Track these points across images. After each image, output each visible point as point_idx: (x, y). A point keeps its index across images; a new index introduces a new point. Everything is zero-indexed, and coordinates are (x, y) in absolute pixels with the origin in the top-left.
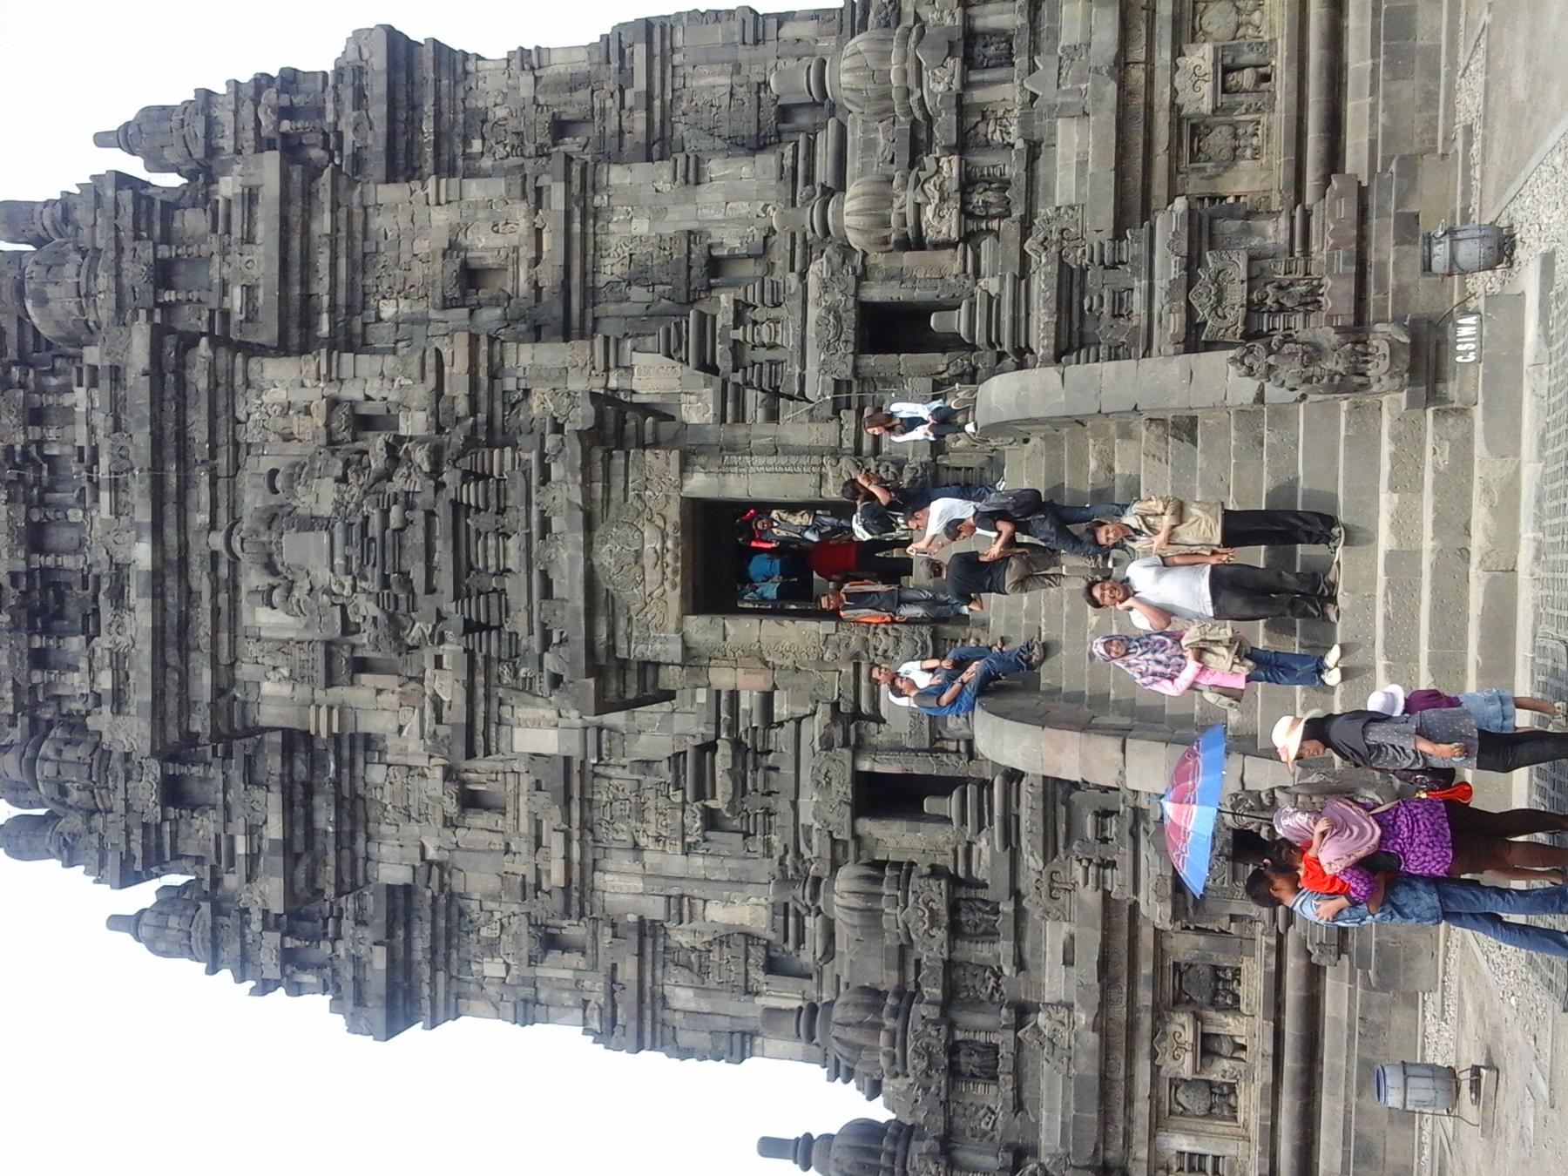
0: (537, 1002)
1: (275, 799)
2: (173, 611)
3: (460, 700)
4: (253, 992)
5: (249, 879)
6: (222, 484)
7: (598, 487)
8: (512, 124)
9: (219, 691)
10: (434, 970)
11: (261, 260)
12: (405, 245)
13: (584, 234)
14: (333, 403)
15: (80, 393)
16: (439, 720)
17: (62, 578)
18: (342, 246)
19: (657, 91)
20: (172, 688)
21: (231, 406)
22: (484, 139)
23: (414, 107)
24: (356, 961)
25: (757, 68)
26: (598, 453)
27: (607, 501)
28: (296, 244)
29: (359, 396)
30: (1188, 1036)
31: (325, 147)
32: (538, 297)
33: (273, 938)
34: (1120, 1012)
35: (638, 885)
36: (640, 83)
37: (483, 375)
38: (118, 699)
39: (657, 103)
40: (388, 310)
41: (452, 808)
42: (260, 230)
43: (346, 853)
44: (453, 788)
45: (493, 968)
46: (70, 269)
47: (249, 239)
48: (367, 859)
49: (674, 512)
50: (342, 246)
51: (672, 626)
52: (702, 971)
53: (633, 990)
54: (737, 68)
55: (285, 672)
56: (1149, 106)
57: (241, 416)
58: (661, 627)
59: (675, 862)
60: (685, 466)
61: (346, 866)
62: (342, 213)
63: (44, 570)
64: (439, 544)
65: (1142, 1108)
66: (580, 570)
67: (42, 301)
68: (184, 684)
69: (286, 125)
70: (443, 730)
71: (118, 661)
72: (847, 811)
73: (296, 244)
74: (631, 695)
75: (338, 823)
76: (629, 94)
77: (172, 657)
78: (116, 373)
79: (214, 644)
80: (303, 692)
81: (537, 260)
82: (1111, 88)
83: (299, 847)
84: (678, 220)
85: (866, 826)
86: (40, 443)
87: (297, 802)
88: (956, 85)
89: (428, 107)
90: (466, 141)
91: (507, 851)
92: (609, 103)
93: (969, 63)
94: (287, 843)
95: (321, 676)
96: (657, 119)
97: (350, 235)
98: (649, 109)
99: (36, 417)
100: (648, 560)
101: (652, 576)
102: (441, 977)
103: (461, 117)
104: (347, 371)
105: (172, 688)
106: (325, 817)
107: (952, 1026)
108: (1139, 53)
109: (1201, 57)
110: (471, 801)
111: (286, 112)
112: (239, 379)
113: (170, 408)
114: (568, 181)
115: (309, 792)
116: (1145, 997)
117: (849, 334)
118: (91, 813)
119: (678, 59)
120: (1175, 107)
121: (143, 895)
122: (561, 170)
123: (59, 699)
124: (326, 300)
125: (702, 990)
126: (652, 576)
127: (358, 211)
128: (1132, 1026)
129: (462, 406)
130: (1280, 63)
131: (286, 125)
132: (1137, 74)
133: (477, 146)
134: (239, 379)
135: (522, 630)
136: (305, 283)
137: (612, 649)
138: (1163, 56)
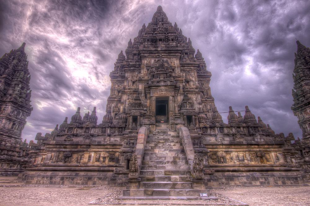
1: (134, 64)
2: (153, 52)
3: (144, 79)
4: (115, 63)
7: (170, 87)
8: (203, 87)
9: (145, 56)
10: (116, 80)
11: (188, 62)
12: (191, 76)
13: (193, 93)
14: (175, 67)
15: (175, 44)
16: (142, 77)
17: (157, 42)
18: (190, 70)
20: (145, 52)
21: (174, 57)
24: (118, 73)
26: (174, 87)
27: (169, 88)
30: (106, 155)
31: (199, 70)
32: (186, 89)
33: (120, 65)
34: (109, 147)
35: (125, 99)
36: (208, 100)
38: (144, 47)
40: (184, 74)
41: (133, 81)
42: (191, 62)
43: (128, 70)
44: (135, 81)
45: (116, 86)
46: (186, 45)
47: (190, 61)
48: (128, 73)
49: (167, 95)
50: (190, 70)
51: (154, 95)
52: (116, 107)
53: (114, 100)
54: (210, 110)
55: (147, 62)
56: (217, 148)
58: (154, 94)
59: (127, 103)
61: (127, 70)
62: (193, 70)
63: (157, 41)
64: (163, 72)
65: (97, 150)
66: (160, 85)
67: (183, 43)
68: (146, 53)
69: (201, 66)
70: (141, 78)
71: (148, 47)
72: (133, 115)
74: (146, 91)
75: (131, 70)
77: (149, 52)
78: (177, 47)
79: (150, 56)
80: (145, 64)
81: (190, 88)
82: (220, 143)
83: (129, 66)
84: (195, 102)
85: (131, 117)
86: (170, 40)
87: (134, 66)
88: (217, 126)
90: (201, 83)
91: (128, 86)
93: (220, 128)
94: (130, 65)
95: (147, 66)
96: (204, 101)
97: (191, 71)
98: (205, 101)
99: (172, 40)
100: (162, 92)
101: (160, 93)
102: (116, 81)
104: (178, 68)
105: (145, 52)
106: (132, 68)
107: (108, 128)
108: (224, 147)
109: (224, 154)
110: (134, 83)
111: (202, 66)
112: (177, 58)
113: (174, 52)
115: (135, 67)
116: (111, 150)
117: (189, 114)
118: (133, 47)
121: (125, 54)
123: (144, 42)
124: (185, 68)
125: (113, 107)
126: (160, 93)
127: (194, 71)
128: (107, 148)
130: (225, 164)
131: (201, 66)
132: (221, 147)
133: (200, 84)
134: (177, 58)
135: (154, 80)
136: (186, 66)
137: (151, 89)
138: (224, 150)
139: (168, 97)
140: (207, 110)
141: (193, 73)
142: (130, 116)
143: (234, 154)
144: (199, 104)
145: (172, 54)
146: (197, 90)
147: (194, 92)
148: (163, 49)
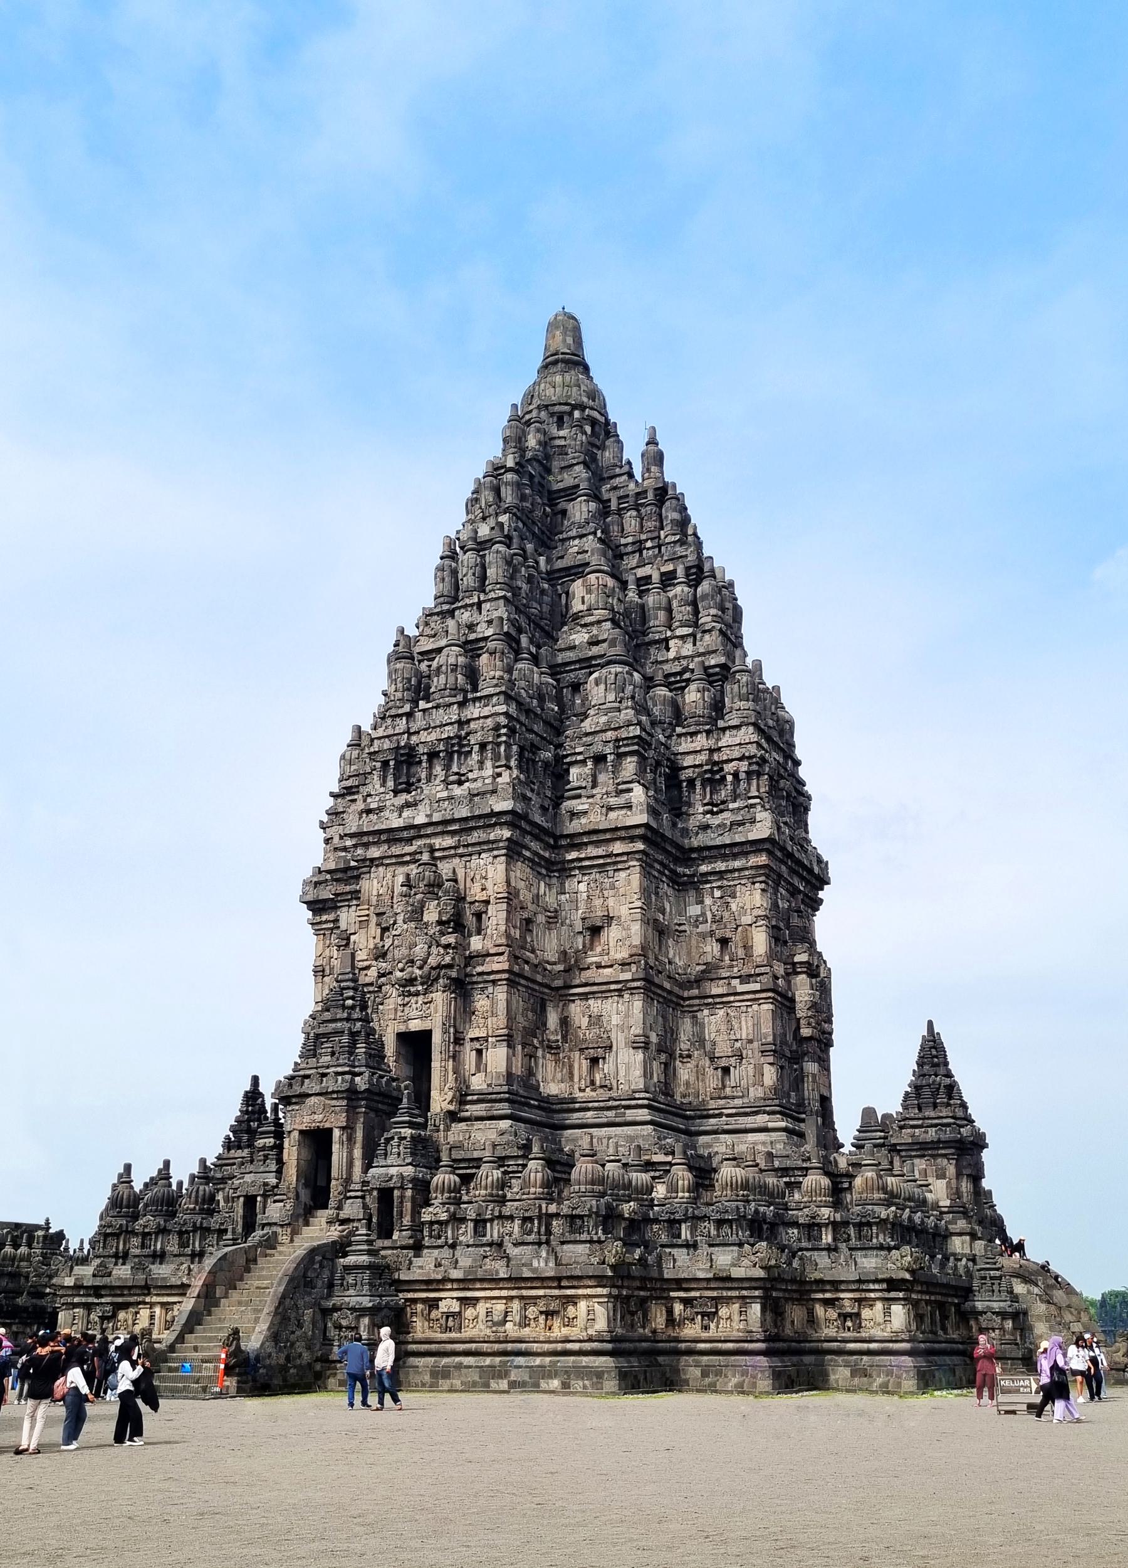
0: (323, 976)
4: (321, 822)
5: (336, 849)
6: (453, 852)
7: (335, 1096)
8: (726, 914)
9: (372, 860)
12: (611, 892)
14: (487, 902)
19: (738, 998)
21: (484, 851)
22: (722, 897)
23: (735, 856)
25: (750, 1052)
28: (608, 836)
29: (490, 914)
36: (741, 988)
37: (492, 977)
39: (732, 998)
40: (583, 887)
42: (612, 815)
48: (349, 906)
49: (327, 1125)
54: (750, 1041)
57: (483, 855)
60: (343, 1128)
69: (729, 778)
73: (608, 836)
76: (735, 982)
80: (374, 900)
82: (440, 1277)
84: (619, 1039)
85: (242, 1199)
89: (737, 864)
90: (719, 887)
92: (736, 970)
96: (725, 999)
103: (731, 883)
111: (736, 775)
112: (496, 853)
114: (633, 980)
119: (755, 1007)
120: (441, 1299)
122: (636, 977)
129: (479, 969)
131: (729, 778)
133: (717, 894)
139: (330, 1131)
140: (738, 1045)
141: (623, 874)
142: (238, 1197)
143: (482, 1307)
144: (634, 1048)
145: (476, 836)
146: (627, 976)
147: (613, 987)
148: (436, 817)
